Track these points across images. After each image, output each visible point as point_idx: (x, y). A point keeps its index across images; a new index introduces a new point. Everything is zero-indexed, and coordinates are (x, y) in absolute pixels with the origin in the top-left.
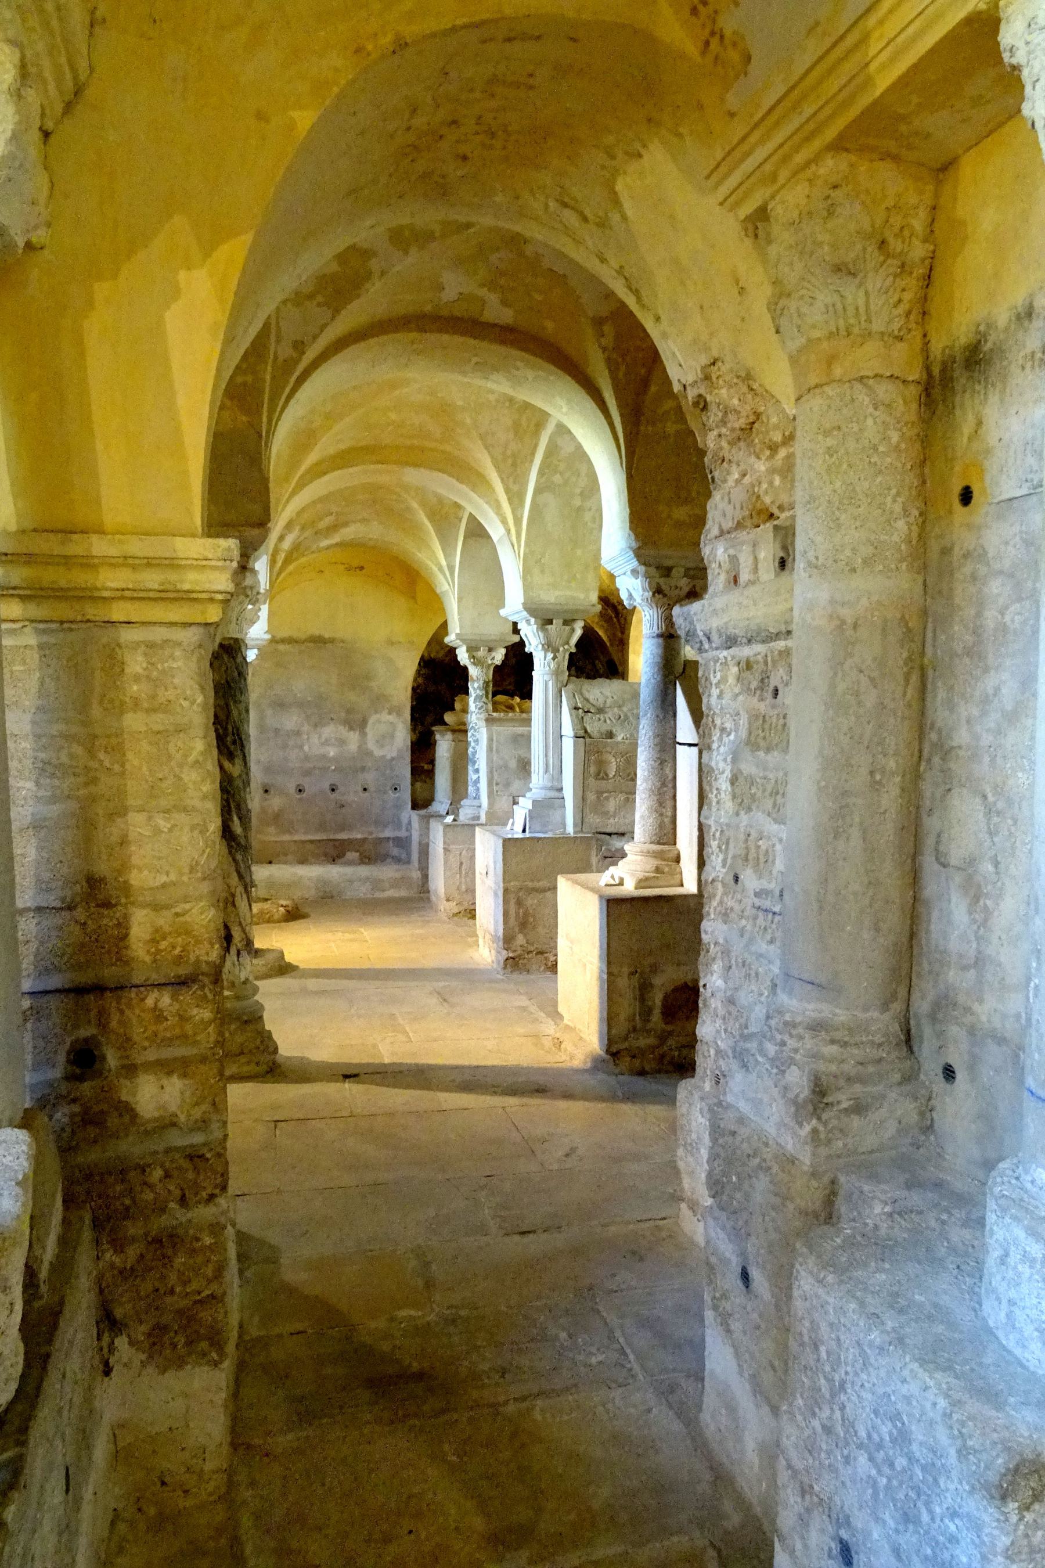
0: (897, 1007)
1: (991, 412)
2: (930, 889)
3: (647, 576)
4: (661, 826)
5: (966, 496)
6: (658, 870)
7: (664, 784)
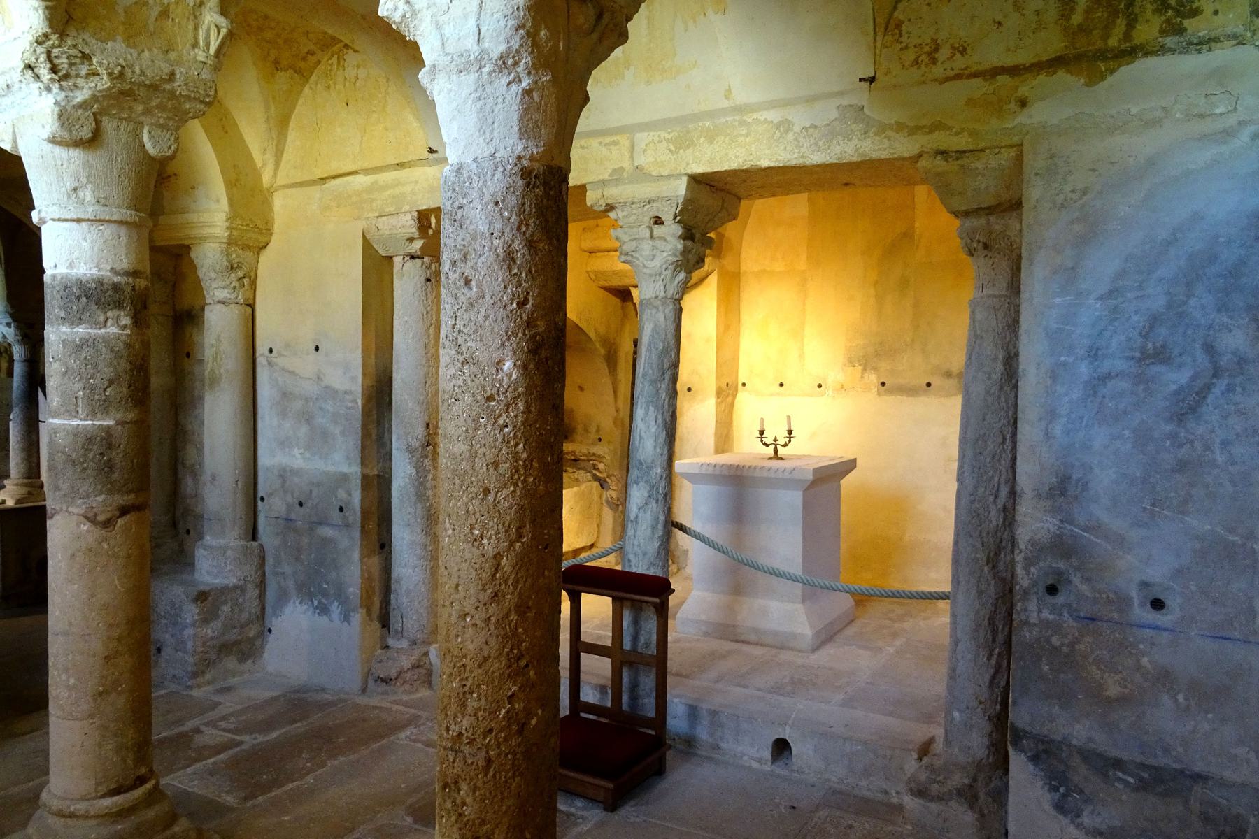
2: (180, 475)
3: (17, 328)
5: (188, 355)
6: (29, 493)
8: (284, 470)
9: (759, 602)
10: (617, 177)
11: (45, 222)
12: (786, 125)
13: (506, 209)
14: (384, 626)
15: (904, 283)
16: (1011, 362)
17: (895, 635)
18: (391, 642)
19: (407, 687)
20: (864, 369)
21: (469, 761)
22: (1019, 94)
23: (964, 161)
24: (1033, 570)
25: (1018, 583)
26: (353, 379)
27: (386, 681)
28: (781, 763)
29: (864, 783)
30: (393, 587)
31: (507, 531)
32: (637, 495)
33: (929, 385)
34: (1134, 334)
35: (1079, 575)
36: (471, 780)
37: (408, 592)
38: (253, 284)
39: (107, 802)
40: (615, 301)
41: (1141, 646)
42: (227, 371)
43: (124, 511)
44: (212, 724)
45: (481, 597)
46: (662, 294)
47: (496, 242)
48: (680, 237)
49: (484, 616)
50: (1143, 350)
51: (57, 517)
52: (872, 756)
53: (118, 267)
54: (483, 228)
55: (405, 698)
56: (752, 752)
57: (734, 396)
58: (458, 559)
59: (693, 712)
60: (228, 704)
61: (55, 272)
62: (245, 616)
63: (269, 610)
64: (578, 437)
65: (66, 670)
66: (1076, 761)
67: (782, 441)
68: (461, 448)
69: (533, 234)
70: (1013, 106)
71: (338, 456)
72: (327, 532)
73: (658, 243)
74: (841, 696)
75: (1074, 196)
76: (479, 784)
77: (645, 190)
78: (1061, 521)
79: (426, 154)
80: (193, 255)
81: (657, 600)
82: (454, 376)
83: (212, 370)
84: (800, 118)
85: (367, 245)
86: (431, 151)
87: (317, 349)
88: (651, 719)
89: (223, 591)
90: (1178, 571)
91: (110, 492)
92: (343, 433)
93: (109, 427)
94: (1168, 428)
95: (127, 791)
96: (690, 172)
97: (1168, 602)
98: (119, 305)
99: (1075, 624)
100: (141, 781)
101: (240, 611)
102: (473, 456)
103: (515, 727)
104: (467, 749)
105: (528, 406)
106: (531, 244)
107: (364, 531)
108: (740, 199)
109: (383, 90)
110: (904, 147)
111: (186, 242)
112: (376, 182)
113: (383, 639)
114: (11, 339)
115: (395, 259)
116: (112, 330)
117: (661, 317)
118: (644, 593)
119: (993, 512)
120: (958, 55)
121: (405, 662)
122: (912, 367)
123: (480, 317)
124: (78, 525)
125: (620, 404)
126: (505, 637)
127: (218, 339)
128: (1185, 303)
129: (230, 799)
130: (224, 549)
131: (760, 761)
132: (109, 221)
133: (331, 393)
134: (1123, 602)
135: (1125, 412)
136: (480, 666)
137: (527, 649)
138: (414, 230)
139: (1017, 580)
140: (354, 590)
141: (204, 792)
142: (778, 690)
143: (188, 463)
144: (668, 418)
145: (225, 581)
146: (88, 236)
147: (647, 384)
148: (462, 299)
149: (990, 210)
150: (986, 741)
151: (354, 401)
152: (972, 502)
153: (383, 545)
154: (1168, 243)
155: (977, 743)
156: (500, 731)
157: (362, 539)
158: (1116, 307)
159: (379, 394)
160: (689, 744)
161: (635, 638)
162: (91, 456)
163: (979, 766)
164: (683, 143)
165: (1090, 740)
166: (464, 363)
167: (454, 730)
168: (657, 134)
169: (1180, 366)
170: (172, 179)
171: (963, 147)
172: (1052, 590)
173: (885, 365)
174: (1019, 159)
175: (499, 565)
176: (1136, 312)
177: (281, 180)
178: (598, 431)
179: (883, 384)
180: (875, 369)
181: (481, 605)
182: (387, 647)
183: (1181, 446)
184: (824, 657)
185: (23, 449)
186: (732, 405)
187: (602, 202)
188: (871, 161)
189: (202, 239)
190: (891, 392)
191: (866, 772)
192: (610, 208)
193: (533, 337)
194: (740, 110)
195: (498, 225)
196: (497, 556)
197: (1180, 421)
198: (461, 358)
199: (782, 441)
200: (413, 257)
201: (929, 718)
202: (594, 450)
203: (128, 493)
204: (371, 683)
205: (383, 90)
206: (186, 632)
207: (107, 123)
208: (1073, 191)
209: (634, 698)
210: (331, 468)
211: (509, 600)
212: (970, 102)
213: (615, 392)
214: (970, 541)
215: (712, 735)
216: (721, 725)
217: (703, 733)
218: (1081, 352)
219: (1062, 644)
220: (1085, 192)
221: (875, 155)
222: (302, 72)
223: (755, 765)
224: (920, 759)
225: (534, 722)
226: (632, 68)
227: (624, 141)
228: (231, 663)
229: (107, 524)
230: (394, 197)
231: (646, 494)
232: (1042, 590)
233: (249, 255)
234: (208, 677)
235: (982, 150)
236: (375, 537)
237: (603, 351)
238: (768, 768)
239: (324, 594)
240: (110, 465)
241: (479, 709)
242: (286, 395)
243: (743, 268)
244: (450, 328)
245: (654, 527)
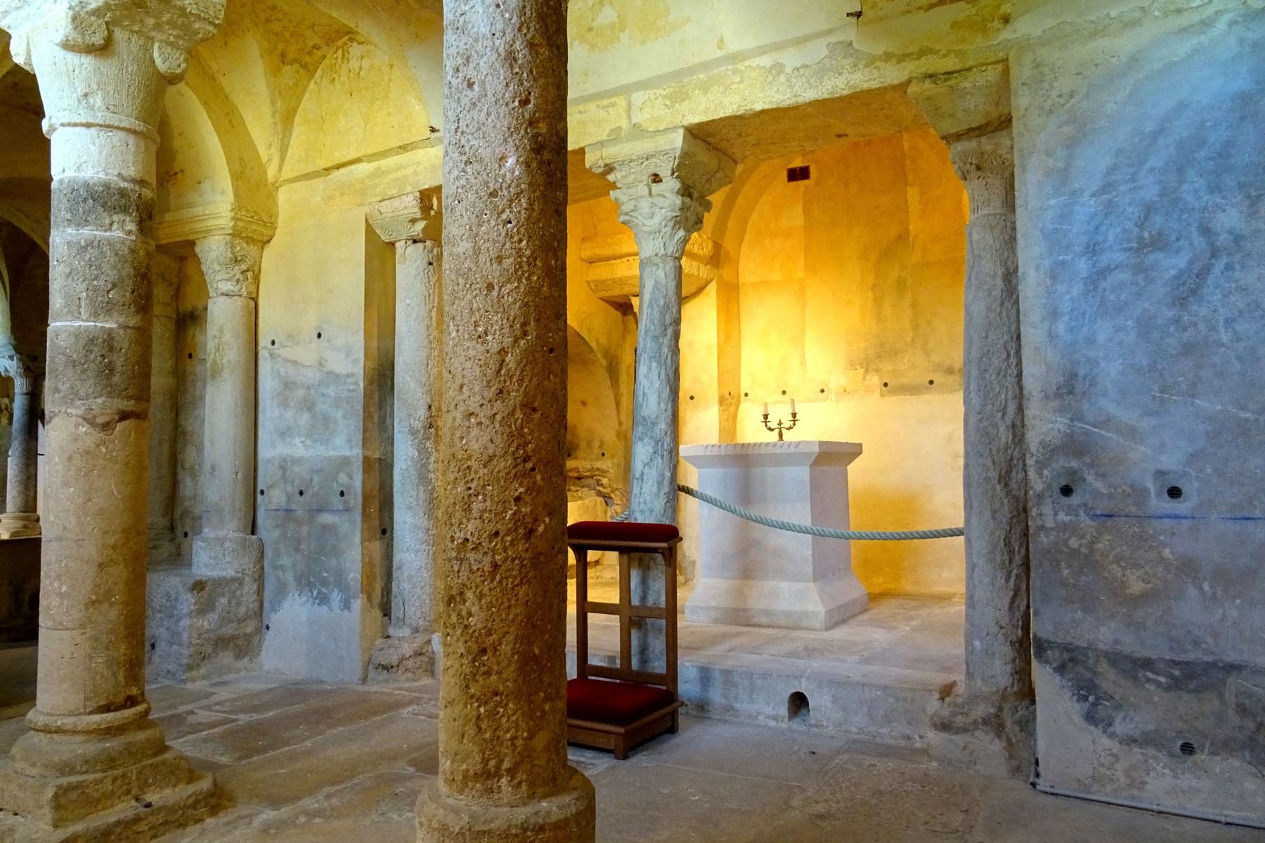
0: (168, 517)
1: (197, 335)
2: (180, 477)
3: (20, 360)
4: (27, 502)
5: (190, 356)
6: (25, 526)
7: (28, 478)
8: (284, 460)
9: (770, 584)
10: (616, 136)
11: (55, 130)
12: (778, 68)
13: (507, 11)
14: (385, 615)
15: (901, 286)
16: (1010, 277)
17: (911, 618)
18: (391, 631)
19: (409, 675)
20: (867, 371)
21: (475, 568)
22: (1001, 12)
23: (952, 82)
24: (1046, 472)
25: (1032, 488)
26: (355, 361)
27: (387, 668)
28: (797, 720)
29: (884, 730)
30: (395, 574)
31: (511, 326)
32: (642, 451)
33: (931, 382)
34: (1129, 225)
35: (1093, 472)
36: (477, 587)
37: (410, 577)
38: (257, 279)
39: (97, 718)
40: (616, 314)
41: (1162, 538)
42: (229, 362)
43: (124, 416)
44: (208, 708)
45: (486, 394)
46: (662, 252)
47: (497, 43)
48: (678, 193)
49: (490, 413)
50: (1140, 239)
51: (56, 420)
52: (891, 700)
53: (125, 173)
54: (484, 30)
55: (406, 685)
56: (769, 710)
57: (737, 406)
58: (462, 359)
59: (705, 675)
60: (223, 694)
61: (62, 176)
62: (242, 610)
63: (266, 604)
64: (581, 454)
65: (58, 577)
66: (1104, 666)
67: (787, 424)
68: (465, 246)
69: (533, 37)
70: (996, 24)
71: (339, 440)
72: (327, 518)
73: (657, 200)
74: (857, 657)
75: (1062, 101)
76: (486, 591)
78: (1072, 420)
79: (428, 134)
80: (197, 250)
81: (664, 545)
82: (457, 178)
83: (214, 361)
84: (791, 59)
85: (370, 230)
86: (433, 130)
87: (319, 336)
88: (661, 676)
89: (220, 582)
90: (1193, 455)
91: (110, 395)
92: (344, 417)
93: (111, 330)
94: (1172, 313)
95: (116, 710)
96: (685, 123)
97: (1185, 489)
98: (125, 210)
99: (1092, 523)
100: (131, 701)
101: (238, 604)
102: (477, 252)
103: (521, 531)
104: (472, 556)
105: (531, 204)
106: (532, 46)
107: (365, 515)
108: (735, 162)
109: (386, 77)
110: (893, 75)
111: (191, 237)
112: (379, 168)
113: (384, 627)
114: (12, 373)
115: (397, 245)
116: (117, 234)
117: (661, 273)
118: (651, 544)
119: (1002, 429)
121: (407, 649)
122: (913, 366)
123: (483, 114)
124: (77, 425)
125: (623, 417)
126: (511, 435)
127: (221, 331)
128: (1176, 189)
129: (224, 760)
130: (221, 541)
131: (776, 718)
132: (118, 128)
133: (333, 377)
134: (1139, 494)
135: (1126, 303)
136: (485, 466)
137: (533, 451)
138: (417, 210)
139: (1031, 504)
140: (354, 576)
141: (198, 755)
142: (791, 654)
143: (187, 466)
144: (671, 375)
145: (223, 574)
146: (97, 141)
147: (649, 340)
148: (465, 101)
149: (980, 131)
150: (1009, 668)
151: (357, 383)
152: (981, 420)
153: (385, 531)
154: (1156, 134)
155: (1000, 672)
156: (507, 535)
157: (363, 522)
158: (1110, 201)
159: (382, 378)
160: (702, 708)
161: (644, 598)
162: (92, 357)
163: (1004, 696)
164: (679, 96)
165: (1117, 642)
166: (468, 162)
167: (460, 536)
168: (652, 92)
169: (1178, 251)
170: (179, 176)
171: (950, 67)
172: (1067, 491)
173: (887, 366)
174: (1006, 73)
175: (503, 361)
176: (1130, 205)
177: (287, 173)
178: (601, 446)
179: (886, 385)
180: (877, 371)
181: (485, 402)
182: (388, 637)
183: (1184, 330)
184: (840, 633)
185: (21, 482)
186: (735, 415)
187: (601, 163)
188: (862, 92)
189: (208, 232)
191: (888, 719)
192: (609, 169)
193: (536, 136)
194: (734, 58)
195: (500, 26)
196: (503, 352)
197: (1182, 305)
198: (464, 158)
199: (787, 424)
200: (415, 242)
201: (948, 669)
202: (598, 464)
203: (131, 398)
204: (372, 673)
205: (386, 77)
206: (179, 618)
207: (119, 34)
208: (1060, 96)
209: (644, 661)
210: (332, 453)
211: (515, 397)
212: (955, 25)
213: (618, 404)
214: (981, 460)
215: (726, 697)
216: (735, 685)
217: (716, 696)
218: (1078, 249)
219: (1081, 545)
220: (1072, 95)
221: (865, 86)
222: (309, 70)
223: (772, 723)
224: (942, 699)
225: (541, 529)
227: (621, 102)
228: (226, 658)
229: (106, 426)
231: (651, 450)
232: (1056, 490)
233: (253, 250)
234: (202, 671)
235: (969, 69)
236: (377, 522)
237: (604, 362)
238: (784, 725)
239: (324, 583)
240: (111, 368)
241: (484, 511)
242: (288, 385)
243: (742, 280)
244: (452, 133)
245: (660, 484)
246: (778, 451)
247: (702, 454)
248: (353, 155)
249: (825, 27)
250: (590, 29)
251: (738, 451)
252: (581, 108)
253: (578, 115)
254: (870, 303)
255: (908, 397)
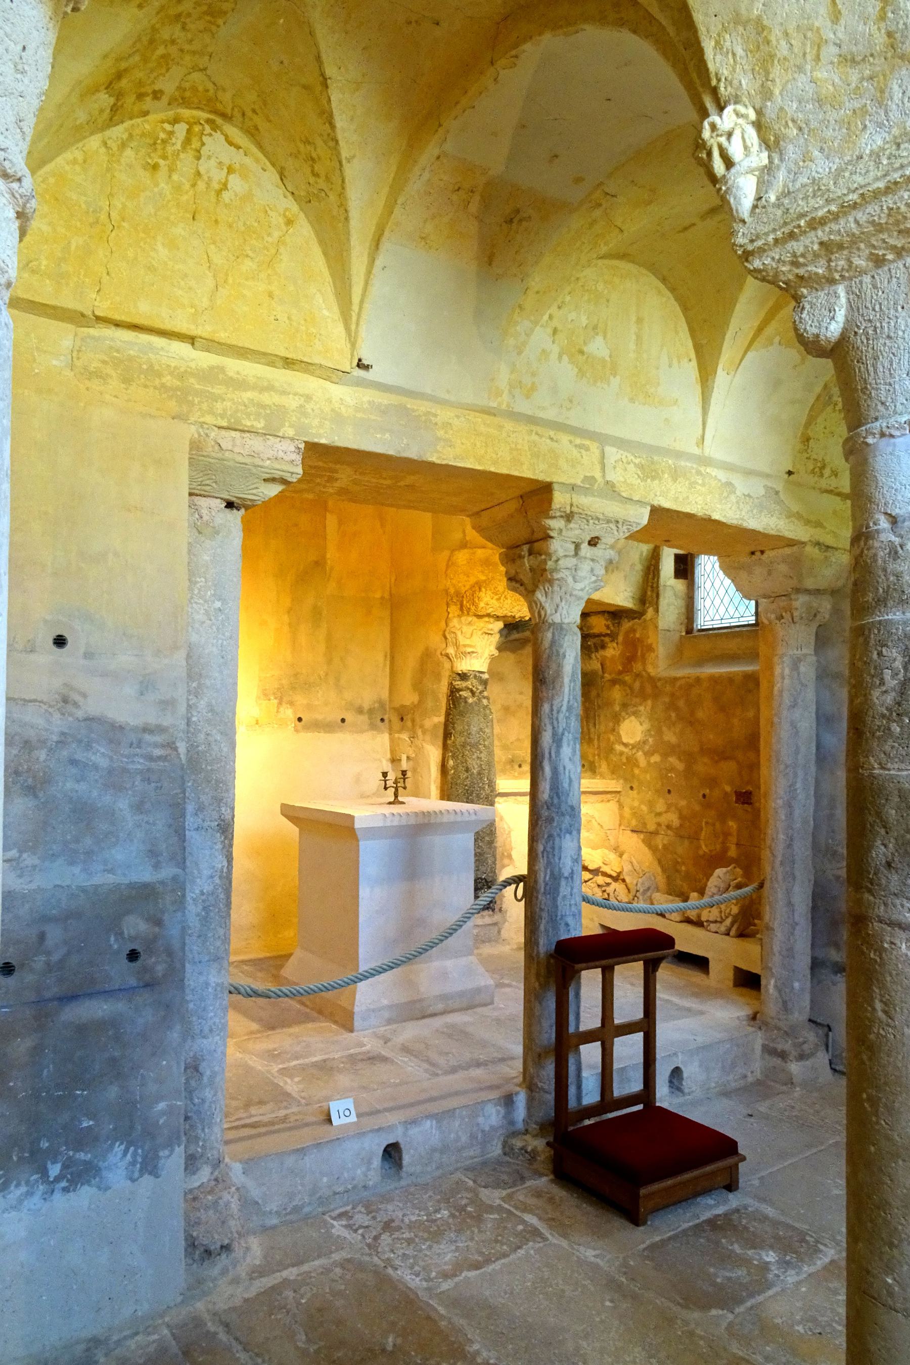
10: (588, 486)
15: (316, 614)
20: (280, 703)
23: (828, 554)
29: (731, 1077)
33: (343, 720)
77: (613, 509)
84: (741, 485)
86: (360, 365)
92: (138, 808)
96: (656, 503)
120: (833, 477)
122: (325, 700)
164: (649, 473)
173: (301, 700)
179: (300, 719)
180: (291, 703)
190: (307, 728)
200: (230, 505)
210: (102, 879)
226: (618, 377)
227: (594, 447)
230: (264, 407)
246: (459, 819)
247: (381, 824)
248: (182, 325)
249: (767, 470)
250: (581, 352)
251: (420, 820)
252: (552, 433)
253: (548, 441)
254: (286, 629)
255: (322, 734)
